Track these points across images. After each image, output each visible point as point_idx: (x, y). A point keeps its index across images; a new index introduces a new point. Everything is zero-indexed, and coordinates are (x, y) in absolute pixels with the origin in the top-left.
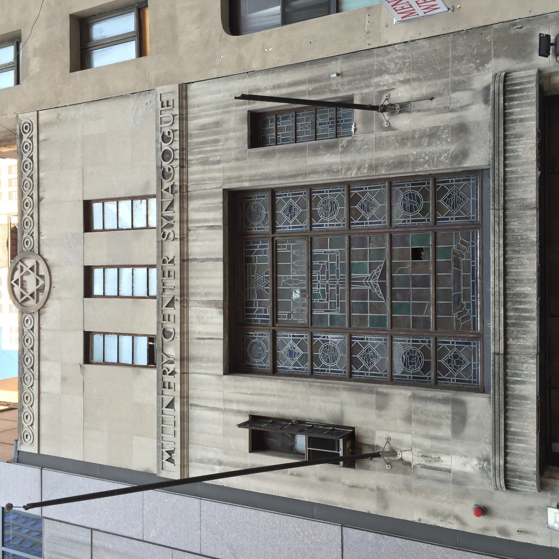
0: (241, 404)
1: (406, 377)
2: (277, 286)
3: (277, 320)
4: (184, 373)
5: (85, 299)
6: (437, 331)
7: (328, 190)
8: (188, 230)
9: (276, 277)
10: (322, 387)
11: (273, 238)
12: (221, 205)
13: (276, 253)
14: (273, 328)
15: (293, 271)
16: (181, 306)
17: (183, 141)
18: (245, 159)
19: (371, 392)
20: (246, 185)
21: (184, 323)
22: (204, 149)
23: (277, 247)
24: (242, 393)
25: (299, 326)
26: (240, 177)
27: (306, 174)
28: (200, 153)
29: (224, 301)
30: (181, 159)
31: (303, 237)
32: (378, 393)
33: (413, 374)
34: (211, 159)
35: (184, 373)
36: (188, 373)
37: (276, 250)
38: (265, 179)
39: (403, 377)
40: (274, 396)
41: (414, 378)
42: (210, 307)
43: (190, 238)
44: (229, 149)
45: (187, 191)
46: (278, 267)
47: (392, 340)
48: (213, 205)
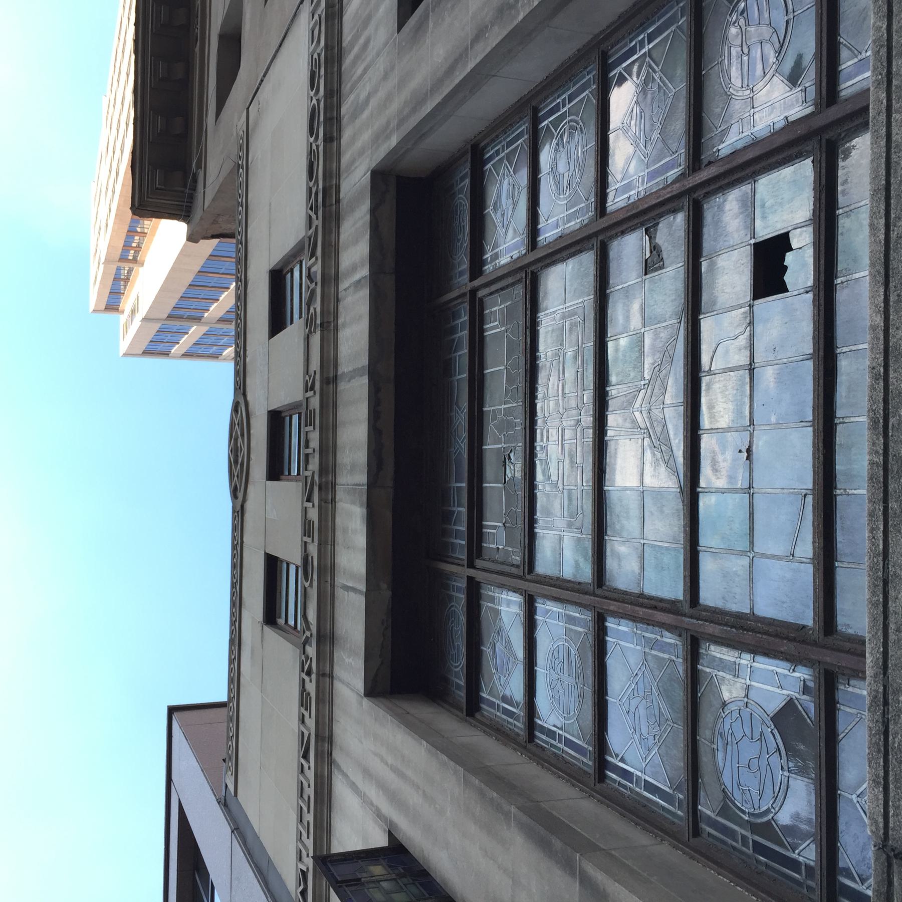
0: (381, 793)
1: (732, 834)
2: (481, 442)
3: (480, 549)
4: (324, 675)
5: (268, 482)
6: (830, 640)
7: (565, 96)
8: (337, 300)
9: (481, 413)
10: (482, 794)
11: (473, 292)
12: (369, 216)
13: (482, 338)
14: (472, 572)
15: (506, 395)
16: (320, 500)
17: (332, 73)
18: (392, 68)
19: (569, 866)
20: (394, 141)
21: (326, 543)
22: (355, 78)
23: (482, 322)
24: (383, 760)
25: (507, 569)
26: (388, 123)
27: (467, 49)
28: (351, 91)
29: (372, 485)
30: (328, 120)
31: (518, 276)
32: (586, 882)
33: (755, 828)
34: (363, 96)
35: (324, 675)
36: (331, 676)
37: (482, 331)
38: (414, 110)
39: (724, 830)
40: (417, 787)
41: (758, 848)
42: (353, 503)
43: (340, 321)
44: (378, 55)
45: (338, 201)
46: (488, 382)
47: (693, 655)
48: (360, 223)
